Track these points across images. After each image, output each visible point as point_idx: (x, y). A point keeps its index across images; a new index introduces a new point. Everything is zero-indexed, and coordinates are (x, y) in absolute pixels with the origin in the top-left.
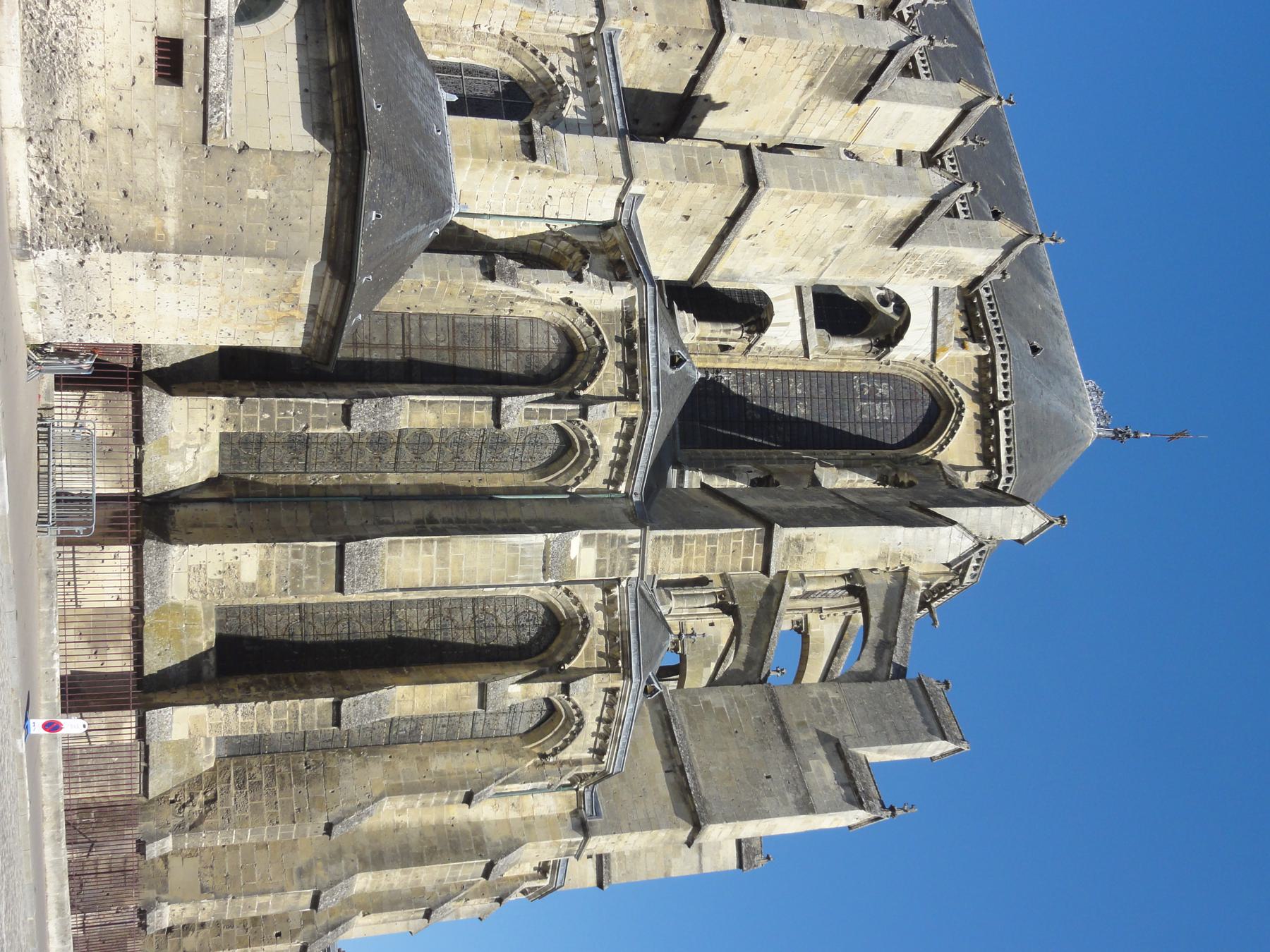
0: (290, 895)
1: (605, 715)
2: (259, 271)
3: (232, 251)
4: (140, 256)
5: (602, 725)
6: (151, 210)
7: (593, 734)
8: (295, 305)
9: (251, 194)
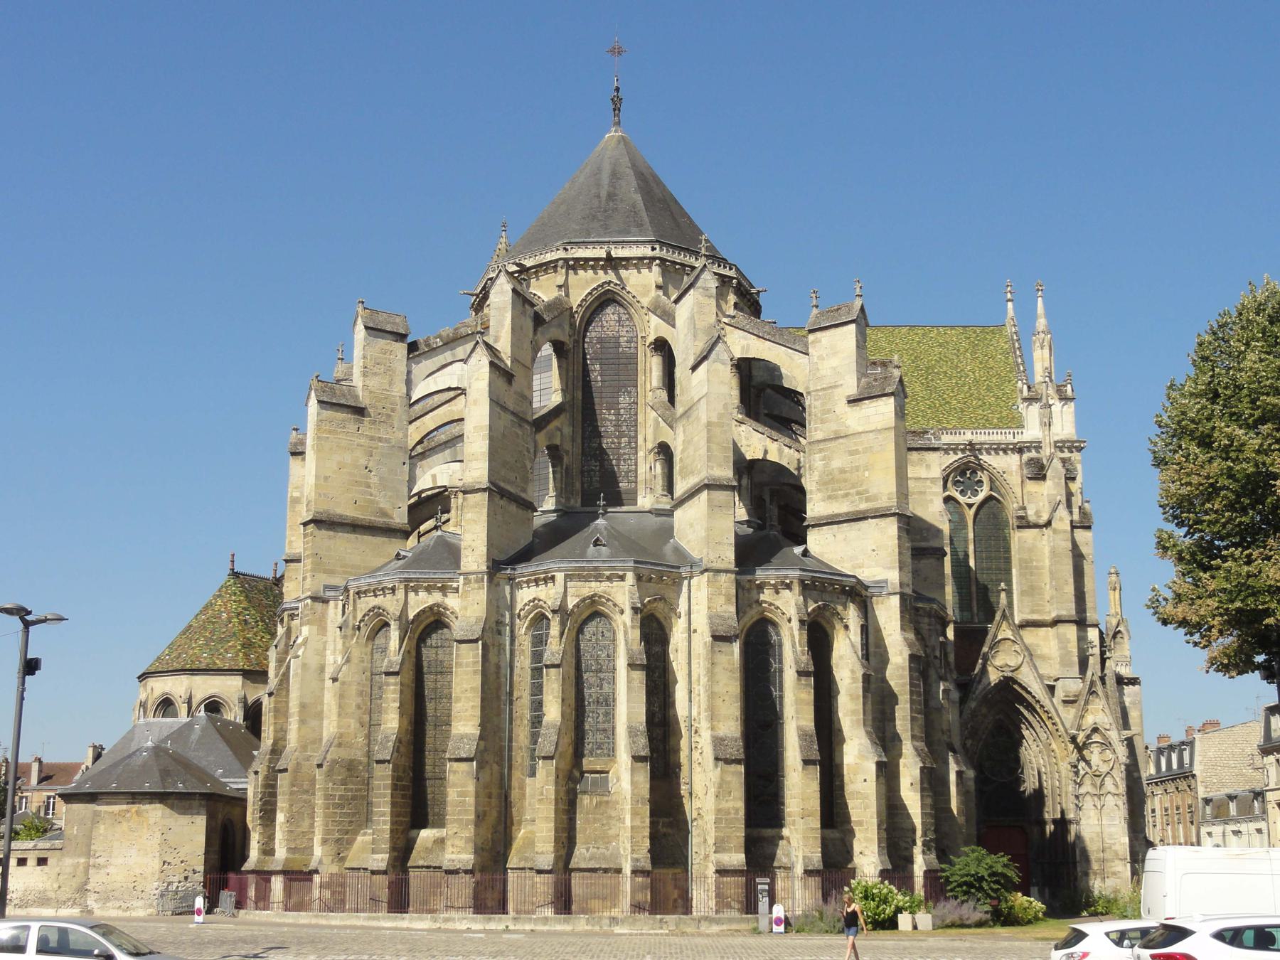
0: (451, 778)
1: (372, 594)
2: (102, 827)
3: (90, 838)
5: (378, 593)
6: (78, 867)
7: (385, 597)
8: (128, 811)
9: (75, 832)
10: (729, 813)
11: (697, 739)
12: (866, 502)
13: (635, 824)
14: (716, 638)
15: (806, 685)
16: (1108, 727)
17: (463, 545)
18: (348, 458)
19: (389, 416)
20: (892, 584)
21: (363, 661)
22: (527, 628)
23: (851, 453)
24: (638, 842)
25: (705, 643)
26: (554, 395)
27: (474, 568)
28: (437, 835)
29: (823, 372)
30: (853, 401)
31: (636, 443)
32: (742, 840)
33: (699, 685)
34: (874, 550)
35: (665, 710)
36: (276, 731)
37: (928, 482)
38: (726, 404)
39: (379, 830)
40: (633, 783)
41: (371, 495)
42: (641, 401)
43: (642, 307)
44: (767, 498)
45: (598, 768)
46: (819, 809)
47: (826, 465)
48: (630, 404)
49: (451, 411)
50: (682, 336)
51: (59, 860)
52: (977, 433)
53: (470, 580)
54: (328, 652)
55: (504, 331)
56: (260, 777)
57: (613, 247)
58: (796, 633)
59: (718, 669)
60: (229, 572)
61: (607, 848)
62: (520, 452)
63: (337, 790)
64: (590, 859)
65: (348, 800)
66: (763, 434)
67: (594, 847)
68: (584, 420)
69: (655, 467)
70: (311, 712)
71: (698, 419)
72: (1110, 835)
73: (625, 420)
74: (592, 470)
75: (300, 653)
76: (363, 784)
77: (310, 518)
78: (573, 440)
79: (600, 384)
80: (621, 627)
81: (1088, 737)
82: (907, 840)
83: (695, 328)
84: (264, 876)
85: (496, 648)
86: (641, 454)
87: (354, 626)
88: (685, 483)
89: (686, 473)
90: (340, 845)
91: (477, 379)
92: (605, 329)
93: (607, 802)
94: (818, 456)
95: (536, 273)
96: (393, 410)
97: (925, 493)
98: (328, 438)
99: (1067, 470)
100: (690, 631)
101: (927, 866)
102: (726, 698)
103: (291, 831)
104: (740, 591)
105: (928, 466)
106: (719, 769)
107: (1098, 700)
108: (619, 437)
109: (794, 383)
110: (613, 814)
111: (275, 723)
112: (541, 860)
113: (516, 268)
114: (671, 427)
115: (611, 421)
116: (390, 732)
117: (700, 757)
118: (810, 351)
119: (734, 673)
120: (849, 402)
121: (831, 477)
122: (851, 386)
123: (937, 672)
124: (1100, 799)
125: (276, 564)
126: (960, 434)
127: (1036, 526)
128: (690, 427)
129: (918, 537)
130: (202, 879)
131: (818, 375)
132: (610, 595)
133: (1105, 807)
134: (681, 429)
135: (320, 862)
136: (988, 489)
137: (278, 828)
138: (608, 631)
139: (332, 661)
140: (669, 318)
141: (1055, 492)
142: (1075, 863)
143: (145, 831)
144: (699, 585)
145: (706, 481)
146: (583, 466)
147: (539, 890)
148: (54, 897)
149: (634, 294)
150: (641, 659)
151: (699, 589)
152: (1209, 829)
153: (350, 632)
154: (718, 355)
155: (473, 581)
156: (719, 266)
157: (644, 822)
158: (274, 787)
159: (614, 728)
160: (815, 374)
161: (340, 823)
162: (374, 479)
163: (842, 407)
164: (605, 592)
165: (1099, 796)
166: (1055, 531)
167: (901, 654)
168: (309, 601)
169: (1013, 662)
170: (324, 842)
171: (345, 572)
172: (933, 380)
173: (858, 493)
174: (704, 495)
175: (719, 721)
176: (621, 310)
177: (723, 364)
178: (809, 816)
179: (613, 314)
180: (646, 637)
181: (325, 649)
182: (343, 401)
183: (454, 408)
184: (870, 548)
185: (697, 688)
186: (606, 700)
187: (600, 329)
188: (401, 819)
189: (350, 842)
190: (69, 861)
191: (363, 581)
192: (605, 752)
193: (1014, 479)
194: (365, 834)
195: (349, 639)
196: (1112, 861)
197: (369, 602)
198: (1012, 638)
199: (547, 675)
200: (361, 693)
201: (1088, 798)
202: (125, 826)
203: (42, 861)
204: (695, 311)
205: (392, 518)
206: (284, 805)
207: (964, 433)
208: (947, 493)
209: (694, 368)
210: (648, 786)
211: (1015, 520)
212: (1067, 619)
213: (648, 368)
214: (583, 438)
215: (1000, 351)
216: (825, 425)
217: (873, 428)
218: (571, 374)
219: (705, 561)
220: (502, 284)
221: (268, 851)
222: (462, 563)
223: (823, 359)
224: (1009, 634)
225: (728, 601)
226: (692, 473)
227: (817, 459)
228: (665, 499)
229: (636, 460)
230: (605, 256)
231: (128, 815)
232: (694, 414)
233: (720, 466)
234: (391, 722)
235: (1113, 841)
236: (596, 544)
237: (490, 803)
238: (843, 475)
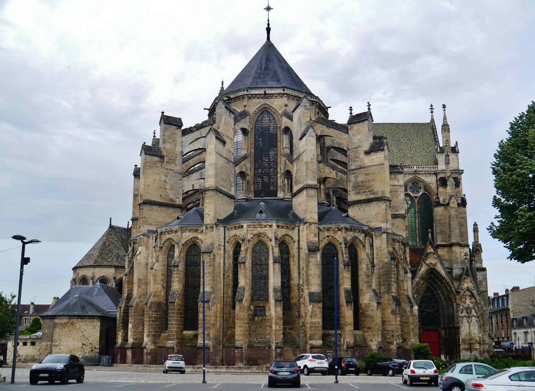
1: (167, 233)
2: (57, 330)
4: (53, 348)
9: (46, 332)
10: (316, 324)
11: (303, 293)
12: (373, 195)
13: (276, 328)
14: (310, 250)
15: (348, 271)
16: (473, 288)
17: (205, 213)
18: (157, 177)
19: (174, 160)
20: (384, 229)
21: (164, 261)
22: (231, 248)
23: (366, 174)
24: (278, 336)
25: (306, 253)
26: (243, 151)
27: (209, 222)
28: (195, 333)
29: (354, 141)
30: (367, 153)
31: (277, 170)
32: (321, 335)
33: (303, 271)
34: (376, 215)
35: (289, 281)
36: (128, 290)
37: (398, 187)
38: (314, 154)
39: (170, 331)
40: (275, 311)
41: (167, 193)
42: (279, 153)
43: (279, 114)
44: (331, 193)
45: (261, 305)
46: (353, 322)
47: (356, 180)
48: (274, 155)
49: (200, 159)
50: (295, 126)
51: (40, 343)
52: (418, 167)
53: (208, 228)
54: (149, 258)
55: (222, 124)
56: (122, 310)
57: (267, 89)
58: (344, 249)
59: (311, 264)
60: (109, 225)
61: (265, 338)
62: (229, 174)
63: (153, 314)
64: (258, 343)
65: (158, 318)
66: (329, 167)
67: (259, 338)
68: (255, 162)
69: (285, 181)
70: (144, 282)
71: (302, 160)
72: (474, 333)
73: (272, 161)
74: (259, 182)
75: (138, 258)
76: (164, 312)
77: (142, 202)
78: (251, 170)
79: (261, 146)
80: (271, 247)
82: (390, 335)
83: (301, 122)
84: (123, 349)
85: (218, 256)
86: (279, 175)
87: (160, 247)
88: (297, 187)
89: (297, 184)
90: (155, 337)
91: (211, 144)
92: (264, 123)
93: (265, 319)
94: (352, 176)
95: (235, 100)
96: (176, 158)
97: (397, 191)
98: (149, 169)
99: (456, 182)
100: (299, 248)
101: (398, 345)
102: (315, 276)
103: (135, 332)
104: (320, 232)
105: (398, 180)
106: (312, 306)
107: (469, 278)
108: (270, 168)
109: (342, 145)
110: (268, 324)
111: (128, 287)
112: (237, 343)
113: (227, 99)
114: (292, 164)
115: (266, 162)
116: (175, 290)
117: (304, 301)
118: (349, 132)
119: (317, 266)
120: (365, 153)
121: (358, 184)
122: (366, 146)
123: (402, 265)
124: (469, 318)
125: (128, 222)
126: (412, 167)
127: (443, 205)
128: (299, 163)
129: (394, 210)
130: (98, 351)
131: (352, 142)
132: (266, 233)
133: (472, 322)
134: (295, 164)
135: (147, 344)
136: (423, 190)
137: (129, 330)
138: (265, 249)
139: (151, 261)
140: (291, 118)
141: (451, 191)
142: (459, 345)
143: (75, 331)
144: (303, 228)
145: (306, 186)
146: (255, 180)
147: (237, 356)
148: (38, 358)
149: (276, 109)
150: (279, 260)
151: (303, 231)
152: (515, 331)
153: (158, 249)
154: (310, 134)
155: (209, 228)
156: (311, 97)
157: (280, 328)
158: (128, 313)
159: (268, 289)
160: (351, 142)
161: (155, 328)
162: (168, 187)
163: (362, 155)
164: (264, 233)
165: (469, 317)
166: (451, 208)
167: (387, 258)
168: (141, 236)
169: (434, 262)
170: (148, 336)
171: (156, 225)
172: (400, 145)
173: (369, 191)
174: (305, 192)
175: (311, 286)
176: (270, 116)
177: (313, 137)
178: (349, 325)
179: (267, 117)
180: (281, 251)
181: (148, 256)
182: (155, 154)
183: (201, 157)
184: (374, 214)
185: (302, 272)
186: (265, 277)
187: (261, 124)
188: (180, 326)
189: (159, 336)
190: (44, 343)
191: (163, 228)
192: (264, 299)
193: (434, 186)
194: (165, 333)
195: (158, 252)
196: (475, 344)
197: (168, 236)
198: (433, 252)
199: (240, 267)
200: (163, 275)
202: (67, 329)
203: (33, 344)
204: (301, 115)
205: (176, 202)
206: (132, 321)
207: (413, 167)
208: (406, 192)
209: (300, 139)
210: (282, 313)
211: (434, 203)
213: (282, 139)
214: (255, 169)
215: (428, 133)
216: (355, 163)
217: (376, 164)
218: (250, 142)
219: (305, 220)
220: (220, 105)
221: (125, 339)
222: (204, 220)
223: (355, 135)
224: (432, 250)
225: (315, 236)
226: (300, 183)
227: (352, 177)
228: (288, 194)
229: (277, 178)
230: (263, 93)
231: (68, 325)
232: (301, 158)
233: (312, 179)
234: (177, 286)
235: (475, 336)
236: (261, 212)
237: (216, 320)
238: (363, 184)
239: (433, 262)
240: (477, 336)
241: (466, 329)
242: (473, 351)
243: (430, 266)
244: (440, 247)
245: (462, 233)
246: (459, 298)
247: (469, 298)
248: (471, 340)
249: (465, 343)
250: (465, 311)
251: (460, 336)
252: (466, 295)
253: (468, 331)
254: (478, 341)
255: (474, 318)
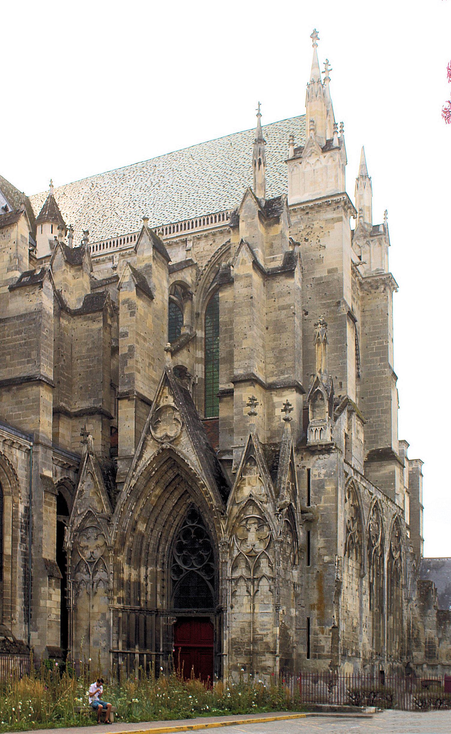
81: (244, 510)
124: (253, 583)
142: (221, 656)
165: (253, 580)
201: (242, 583)
212: (243, 378)
224: (170, 401)
235: (265, 632)
239: (172, 434)
240: (269, 632)
241: (244, 614)
242: (257, 673)
243: (163, 443)
244: (225, 396)
245: (281, 351)
246: (227, 526)
247: (256, 526)
248: (255, 642)
249: (238, 653)
250: (243, 565)
251: (226, 632)
252: (247, 519)
253: (248, 618)
254: (272, 645)
255: (264, 582)
